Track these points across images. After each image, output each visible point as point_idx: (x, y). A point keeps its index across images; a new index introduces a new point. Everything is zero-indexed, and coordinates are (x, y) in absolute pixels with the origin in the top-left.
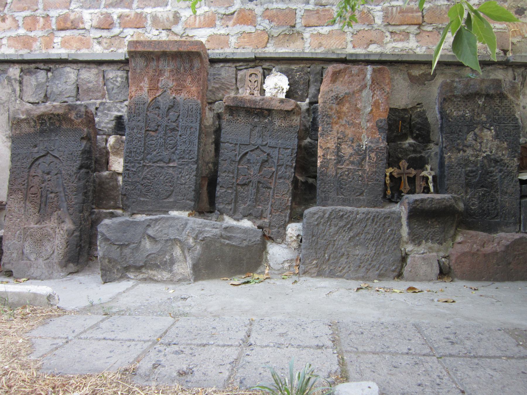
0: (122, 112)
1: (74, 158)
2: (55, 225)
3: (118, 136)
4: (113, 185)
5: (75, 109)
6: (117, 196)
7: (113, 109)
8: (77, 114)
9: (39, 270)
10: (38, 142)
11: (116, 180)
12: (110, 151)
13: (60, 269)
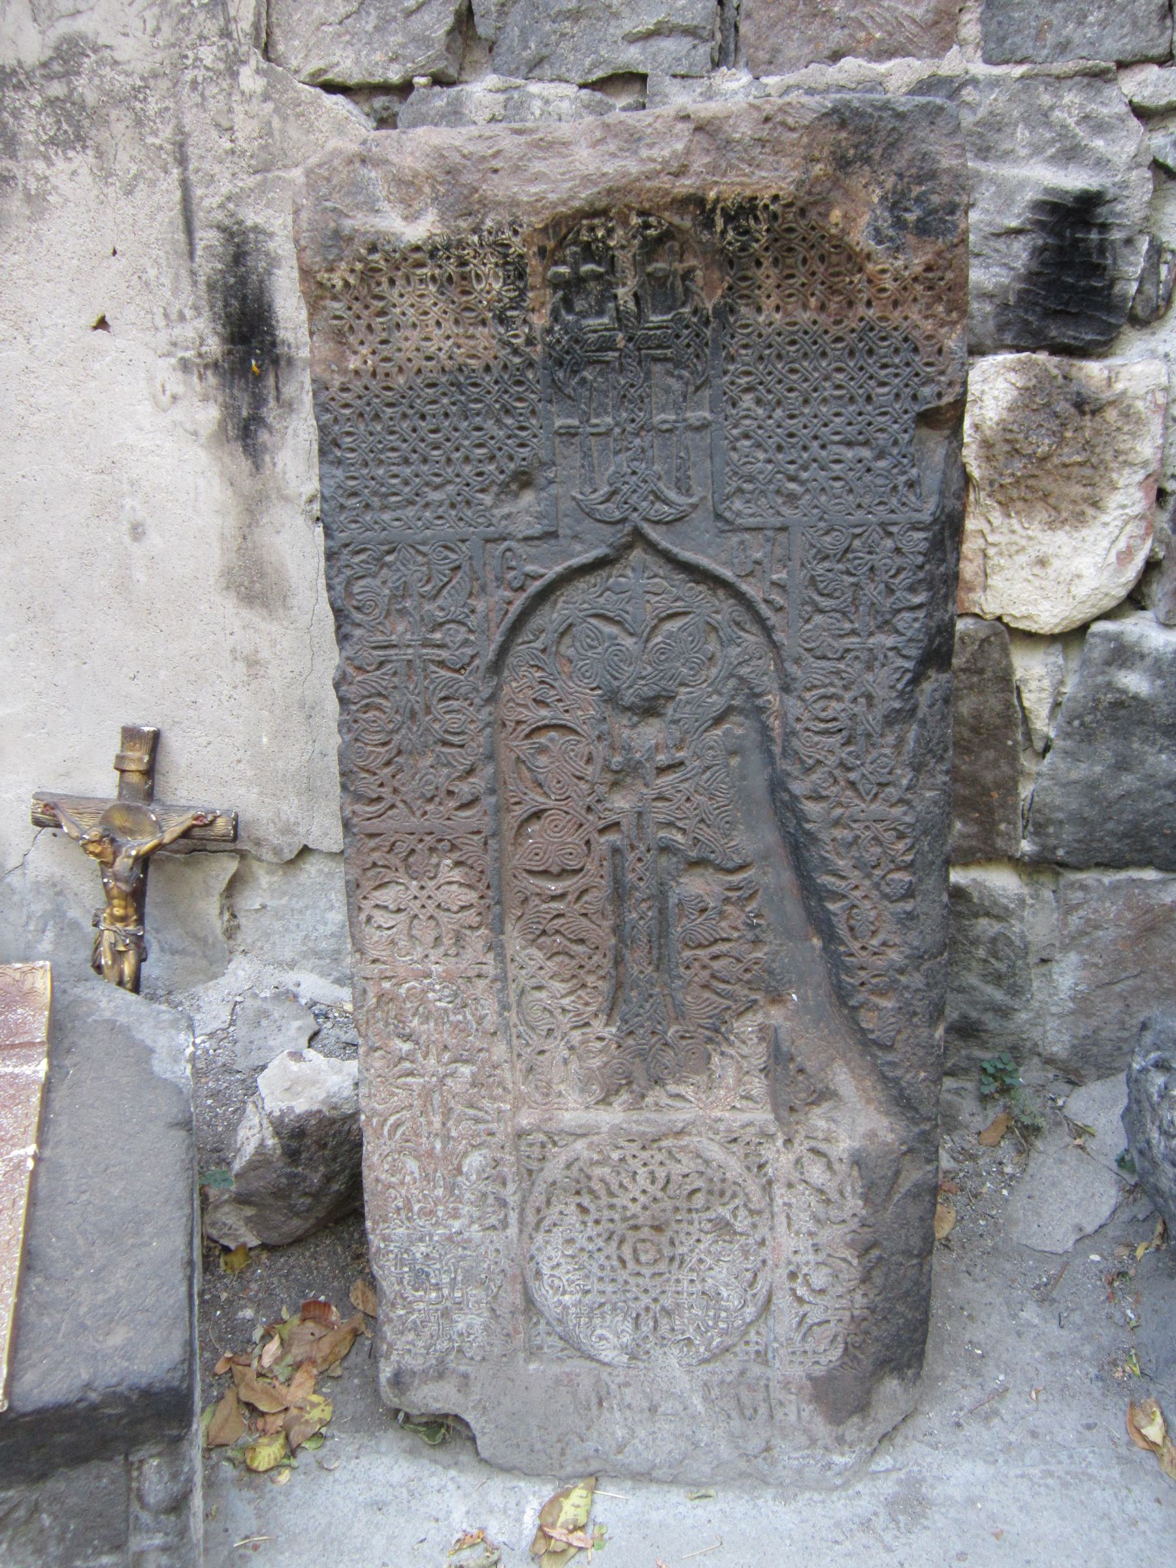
0: (1101, 163)
1: (872, 591)
2: (763, 1116)
3: (1042, 357)
4: (978, 716)
5: (886, 156)
6: (998, 786)
7: (1021, 133)
8: (895, 204)
9: (665, 1427)
10: (539, 447)
11: (1006, 682)
12: (975, 472)
13: (821, 1428)
